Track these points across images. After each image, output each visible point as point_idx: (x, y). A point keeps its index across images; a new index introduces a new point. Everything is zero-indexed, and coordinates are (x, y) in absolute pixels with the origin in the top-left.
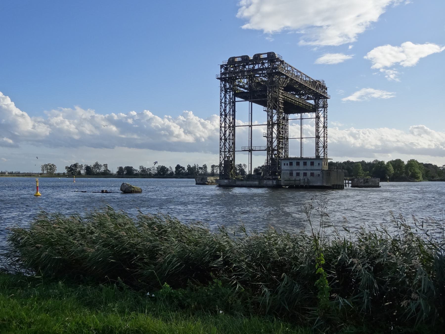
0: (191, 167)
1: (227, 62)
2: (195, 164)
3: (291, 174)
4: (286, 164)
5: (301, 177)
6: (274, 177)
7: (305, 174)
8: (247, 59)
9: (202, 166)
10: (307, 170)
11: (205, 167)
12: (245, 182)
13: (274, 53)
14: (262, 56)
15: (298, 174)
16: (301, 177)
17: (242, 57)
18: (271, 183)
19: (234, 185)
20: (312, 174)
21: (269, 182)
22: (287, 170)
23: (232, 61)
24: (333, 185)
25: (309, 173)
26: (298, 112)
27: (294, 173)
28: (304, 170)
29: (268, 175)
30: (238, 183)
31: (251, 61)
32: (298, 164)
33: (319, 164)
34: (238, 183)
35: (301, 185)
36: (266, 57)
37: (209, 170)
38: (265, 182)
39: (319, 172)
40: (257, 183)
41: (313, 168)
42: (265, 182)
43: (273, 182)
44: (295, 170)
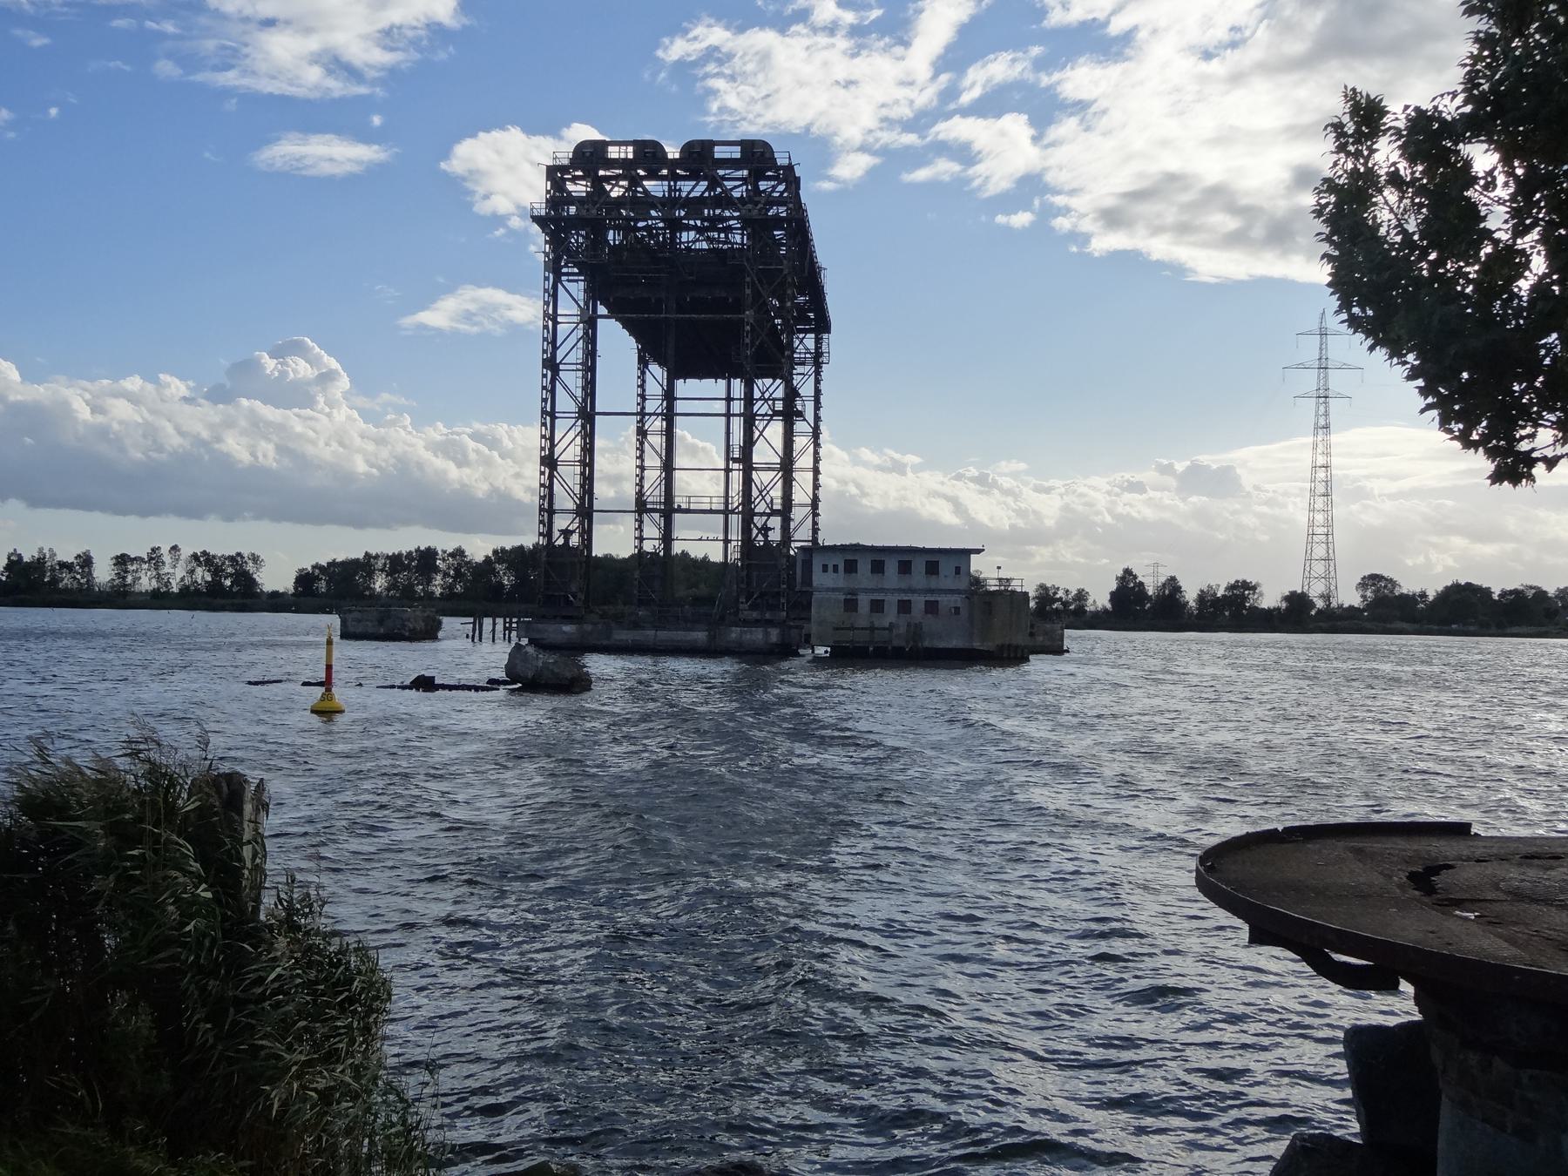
0: (26, 559)
1: (571, 156)
2: (41, 550)
3: (851, 605)
4: (830, 568)
5: (890, 616)
6: (768, 616)
7: (904, 607)
8: (654, 154)
9: (70, 559)
10: (912, 591)
11: (86, 561)
12: (651, 633)
13: (765, 145)
14: (720, 153)
15: (877, 606)
16: (890, 616)
17: (640, 145)
18: (760, 636)
19: (605, 642)
20: (932, 608)
21: (751, 633)
22: (834, 590)
24: (1001, 648)
25: (919, 602)
26: (715, 375)
27: (864, 601)
28: (900, 590)
29: (746, 606)
30: (624, 637)
31: (673, 164)
32: (878, 568)
33: (958, 571)
34: (623, 636)
35: (894, 648)
36: (738, 156)
37: (103, 573)
38: (734, 635)
39: (956, 600)
40: (700, 636)
41: (934, 583)
42: (734, 635)
43: (767, 634)
44: (866, 591)
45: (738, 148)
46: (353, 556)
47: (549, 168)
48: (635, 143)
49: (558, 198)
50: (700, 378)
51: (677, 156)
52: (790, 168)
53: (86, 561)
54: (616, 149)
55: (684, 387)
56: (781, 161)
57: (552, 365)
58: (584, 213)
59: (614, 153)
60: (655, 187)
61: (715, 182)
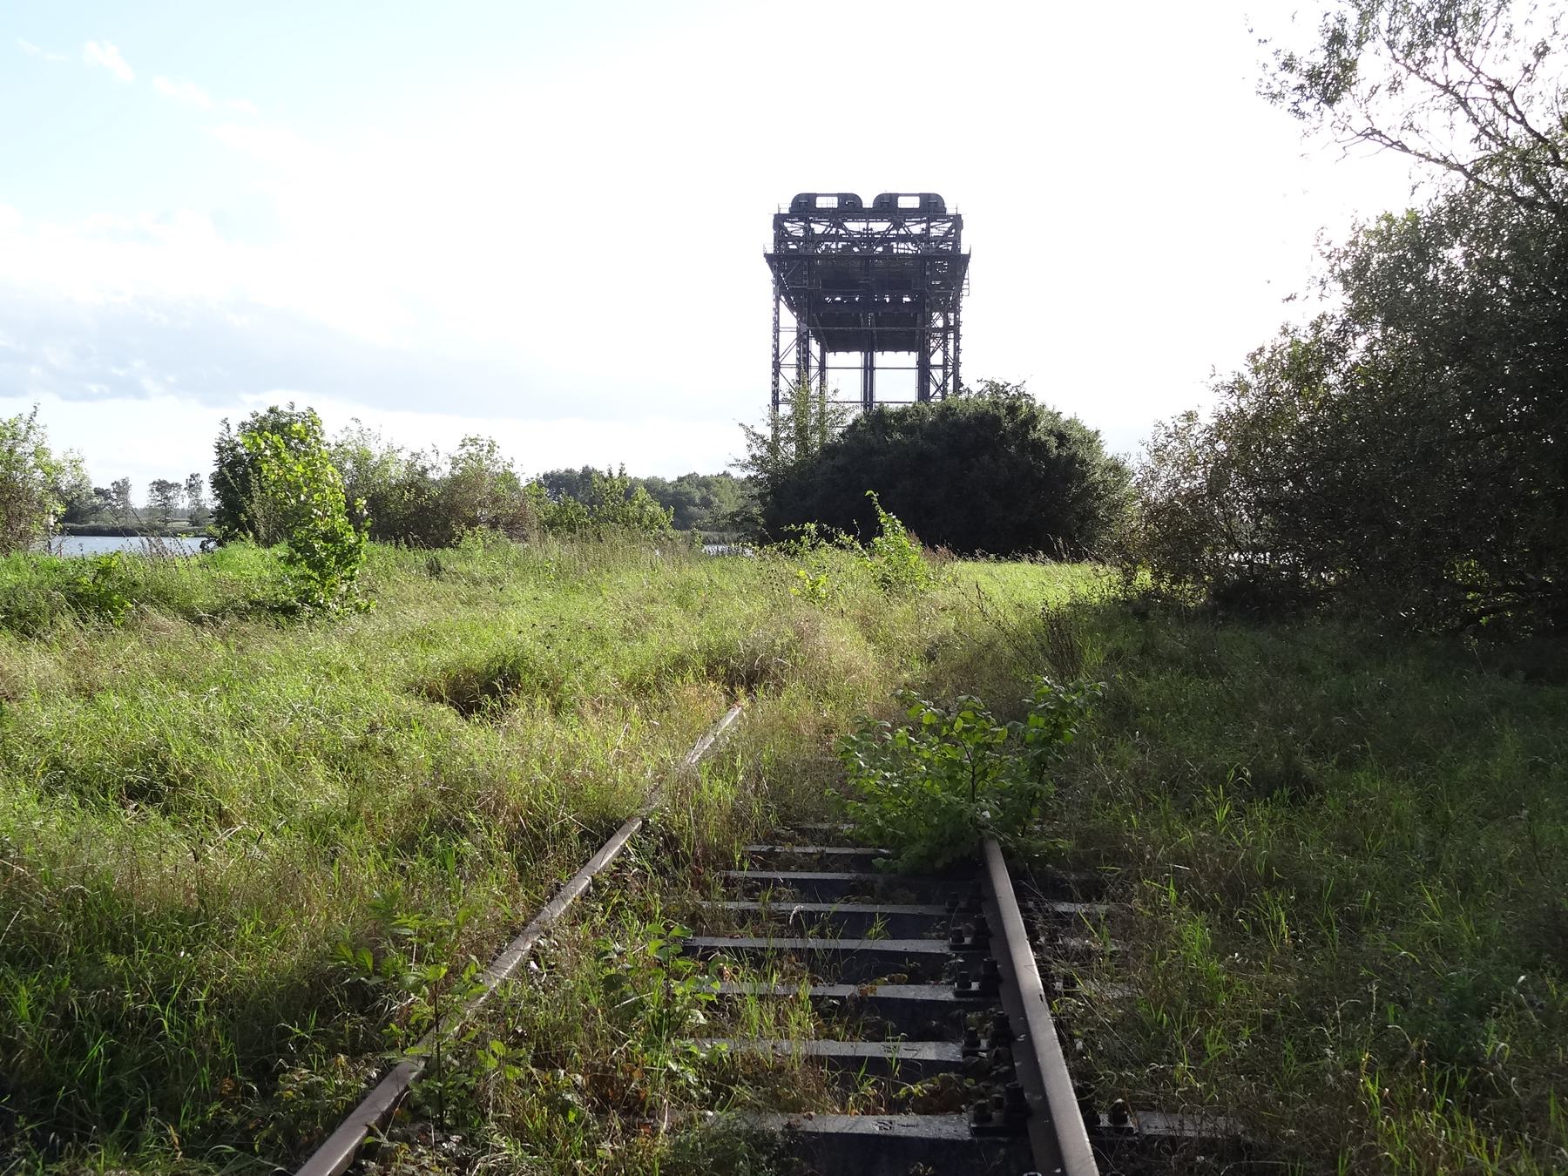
11: (122, 488)
13: (938, 197)
14: (903, 203)
17: (843, 197)
23: (804, 207)
36: (917, 206)
37: (140, 498)
47: (775, 215)
48: (839, 196)
49: (781, 236)
50: (848, 350)
51: (867, 206)
53: (122, 488)
55: (833, 359)
56: (950, 211)
57: (777, 366)
58: (802, 251)
59: (821, 203)
60: (855, 226)
61: (897, 226)
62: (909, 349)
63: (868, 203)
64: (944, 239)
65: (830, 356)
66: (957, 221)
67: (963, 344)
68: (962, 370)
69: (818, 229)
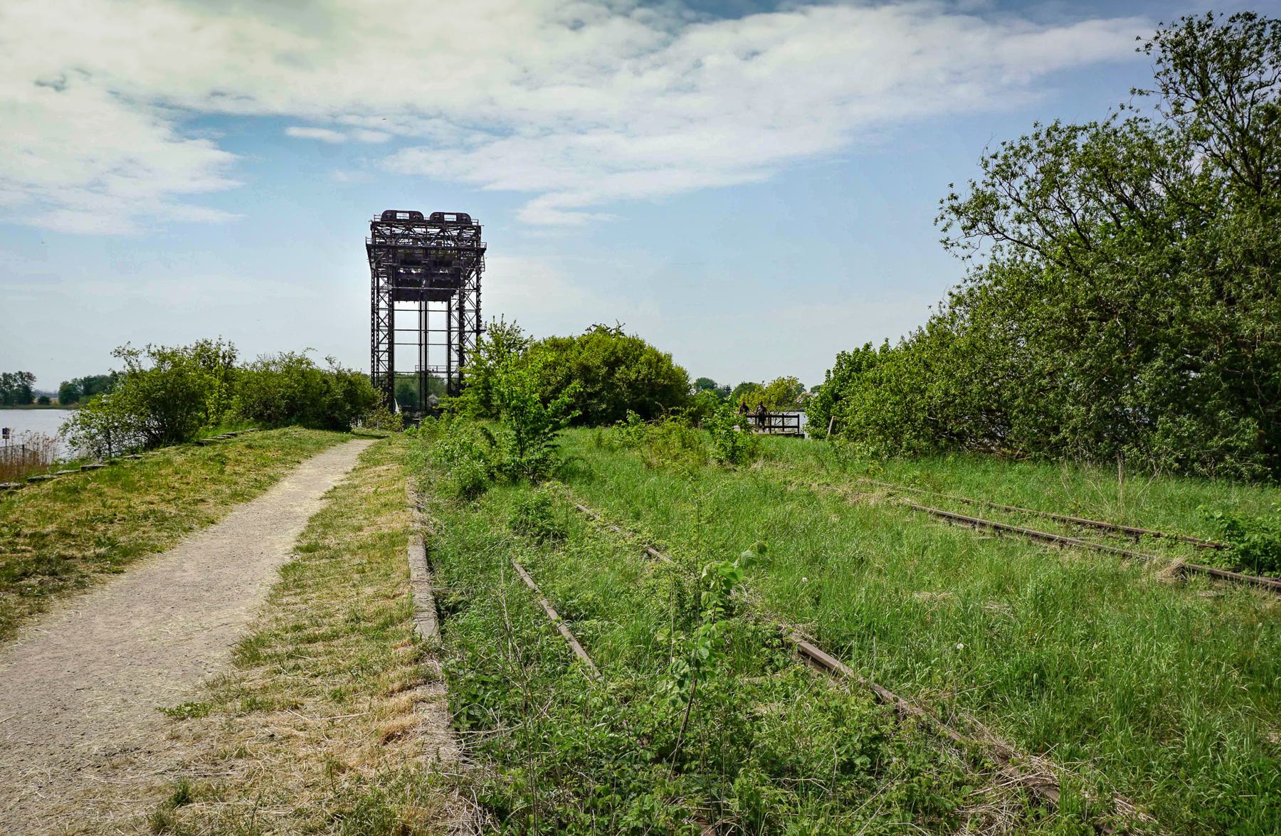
26: (415, 300)
45: (455, 217)
46: (101, 374)
50: (407, 300)
52: (479, 227)
54: (401, 214)
55: (397, 305)
59: (399, 216)
60: (418, 230)
62: (443, 300)
63: (427, 216)
64: (470, 239)
65: (396, 303)
66: (478, 229)
67: (482, 297)
68: (482, 313)
69: (398, 231)
